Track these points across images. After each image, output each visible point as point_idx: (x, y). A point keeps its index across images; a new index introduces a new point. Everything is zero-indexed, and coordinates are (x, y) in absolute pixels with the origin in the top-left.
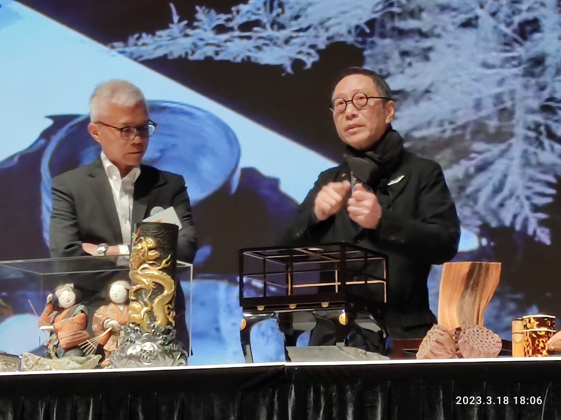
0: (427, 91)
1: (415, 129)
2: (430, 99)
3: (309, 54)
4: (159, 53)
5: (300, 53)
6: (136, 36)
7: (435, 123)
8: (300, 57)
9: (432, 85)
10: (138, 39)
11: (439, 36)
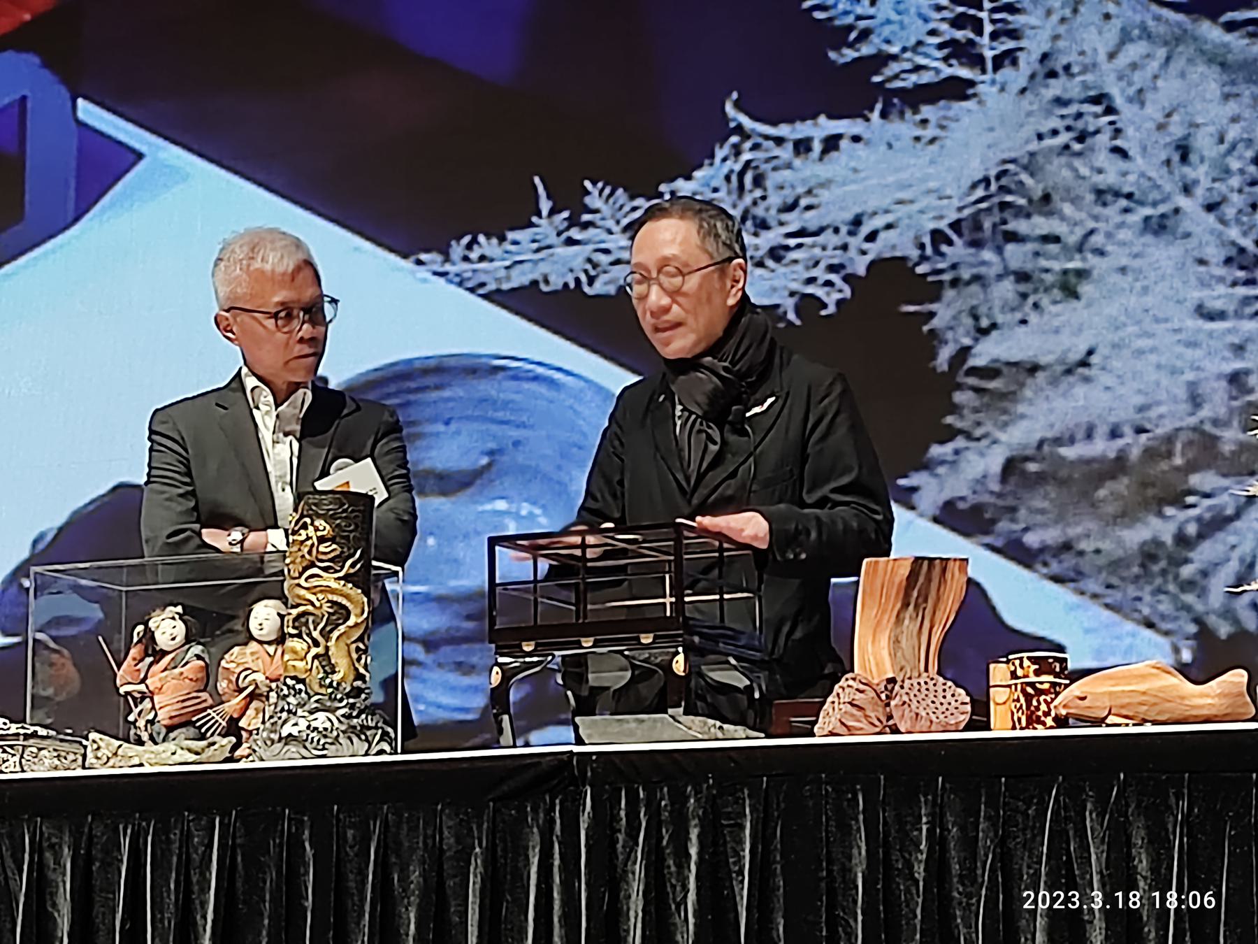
0: (1084, 363)
1: (1058, 441)
2: (1087, 380)
3: (828, 283)
4: (519, 278)
5: (811, 281)
6: (466, 240)
7: (1102, 430)
8: (810, 290)
9: (1090, 352)
10: (469, 247)
11: (1100, 252)
